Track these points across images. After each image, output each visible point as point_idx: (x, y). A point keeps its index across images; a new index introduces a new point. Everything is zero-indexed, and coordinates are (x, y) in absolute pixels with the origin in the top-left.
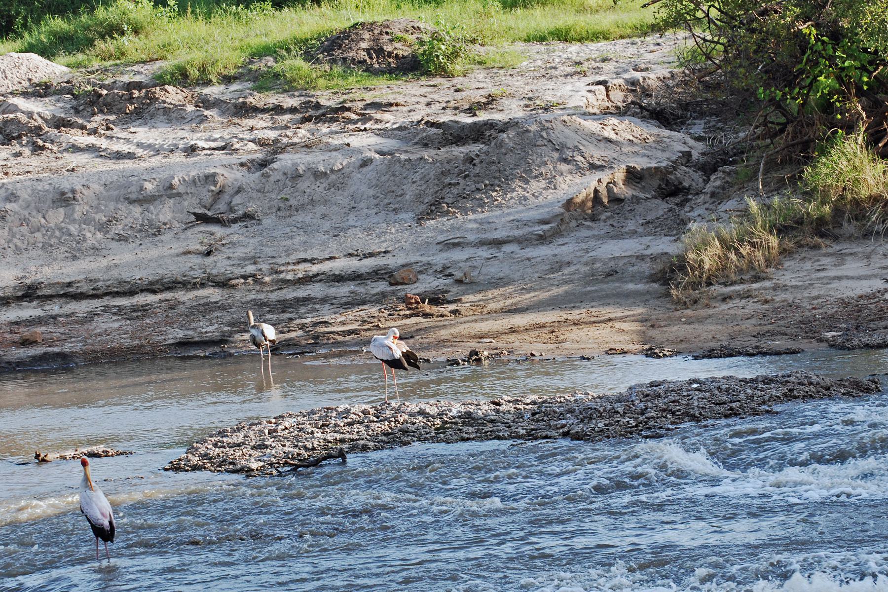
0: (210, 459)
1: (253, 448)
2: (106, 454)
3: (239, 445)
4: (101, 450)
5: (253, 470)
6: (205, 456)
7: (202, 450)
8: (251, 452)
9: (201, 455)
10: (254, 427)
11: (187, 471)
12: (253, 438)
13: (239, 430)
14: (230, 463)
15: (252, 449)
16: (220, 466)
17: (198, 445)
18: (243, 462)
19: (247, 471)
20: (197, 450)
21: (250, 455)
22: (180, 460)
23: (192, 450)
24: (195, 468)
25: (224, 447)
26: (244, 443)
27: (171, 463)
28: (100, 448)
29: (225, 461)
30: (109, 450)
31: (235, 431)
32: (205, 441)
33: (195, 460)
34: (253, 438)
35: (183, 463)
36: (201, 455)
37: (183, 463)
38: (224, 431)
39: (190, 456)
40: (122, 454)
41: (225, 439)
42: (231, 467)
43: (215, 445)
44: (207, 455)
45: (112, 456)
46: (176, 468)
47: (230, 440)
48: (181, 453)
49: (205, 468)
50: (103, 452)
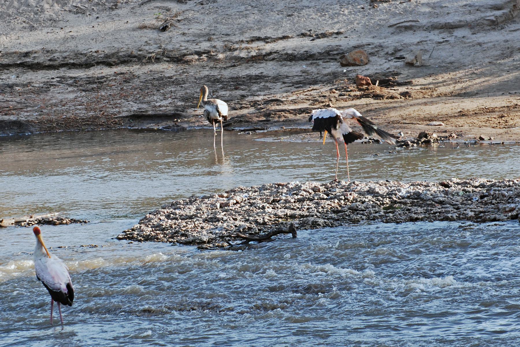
0: (163, 230)
1: (205, 220)
2: (61, 222)
3: (191, 217)
5: (204, 242)
6: (158, 227)
7: (155, 221)
8: (204, 225)
9: (154, 226)
10: (206, 200)
11: (140, 241)
12: (205, 211)
13: (191, 202)
14: (183, 235)
15: (204, 221)
16: (172, 237)
17: (151, 216)
18: (195, 234)
19: (198, 243)
20: (150, 221)
21: (202, 228)
22: (133, 230)
23: (145, 221)
24: (147, 238)
25: (176, 219)
26: (196, 216)
27: (125, 232)
29: (177, 232)
31: (187, 204)
32: (158, 213)
33: (148, 230)
34: (205, 211)
35: (136, 233)
36: (154, 226)
37: (136, 233)
38: (177, 203)
39: (143, 226)
41: (177, 211)
42: (183, 238)
43: (168, 217)
44: (159, 226)
45: (66, 224)
46: (129, 237)
47: (182, 212)
49: (157, 239)
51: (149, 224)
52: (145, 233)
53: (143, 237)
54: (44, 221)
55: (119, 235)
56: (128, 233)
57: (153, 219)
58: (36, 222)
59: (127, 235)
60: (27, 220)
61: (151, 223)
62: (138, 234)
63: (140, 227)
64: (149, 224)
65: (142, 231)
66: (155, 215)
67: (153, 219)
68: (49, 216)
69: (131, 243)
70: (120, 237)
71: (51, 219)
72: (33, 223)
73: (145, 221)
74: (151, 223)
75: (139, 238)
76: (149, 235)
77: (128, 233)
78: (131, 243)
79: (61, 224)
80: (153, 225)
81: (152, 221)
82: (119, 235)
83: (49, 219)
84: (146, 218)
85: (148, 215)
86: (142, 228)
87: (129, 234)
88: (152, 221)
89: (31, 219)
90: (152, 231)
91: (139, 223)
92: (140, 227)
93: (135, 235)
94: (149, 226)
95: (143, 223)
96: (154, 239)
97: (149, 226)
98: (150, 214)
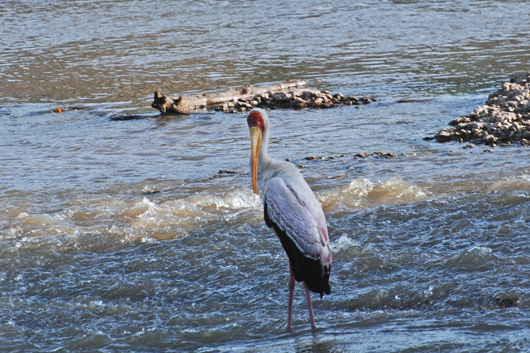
4: (298, 92)
11: (490, 143)
17: (516, 86)
22: (474, 118)
23: (502, 98)
24: (506, 137)
27: (454, 123)
28: (297, 88)
30: (317, 92)
33: (508, 119)
35: (480, 125)
37: (480, 125)
39: (496, 110)
40: (346, 101)
45: (323, 106)
46: (464, 134)
48: (477, 102)
50: (304, 96)
51: (511, 105)
52: (500, 124)
53: (497, 135)
54: (274, 100)
55: (441, 131)
56: (462, 124)
57: (518, 93)
58: (255, 102)
59: (459, 129)
60: (236, 99)
61: (515, 103)
62: (484, 128)
63: (490, 111)
64: (511, 105)
65: (495, 120)
66: (523, 84)
67: (518, 93)
68: (284, 88)
69: (470, 147)
70: (444, 134)
71: (289, 96)
72: (249, 105)
73: (502, 98)
74: (515, 103)
75: (488, 137)
76: (511, 129)
77: (462, 124)
78: (470, 147)
79: (313, 106)
80: (520, 105)
81: (517, 97)
82: (441, 131)
83: (283, 95)
84: (503, 91)
85: (507, 85)
86: (494, 113)
87: (465, 128)
88: (517, 97)
89: (244, 97)
90: (518, 120)
91: (487, 103)
92: (490, 111)
93: (479, 131)
94: (511, 109)
95: (497, 103)
96: (522, 137)
97: (511, 109)
98: (512, 81)
